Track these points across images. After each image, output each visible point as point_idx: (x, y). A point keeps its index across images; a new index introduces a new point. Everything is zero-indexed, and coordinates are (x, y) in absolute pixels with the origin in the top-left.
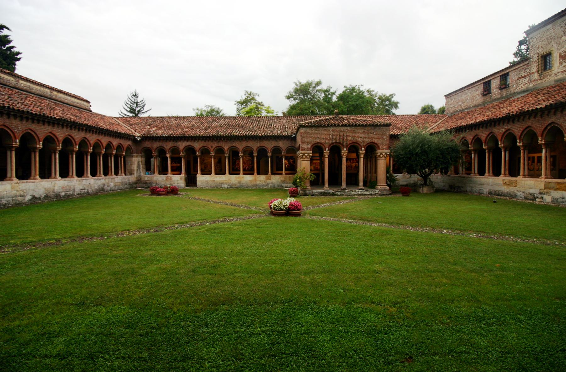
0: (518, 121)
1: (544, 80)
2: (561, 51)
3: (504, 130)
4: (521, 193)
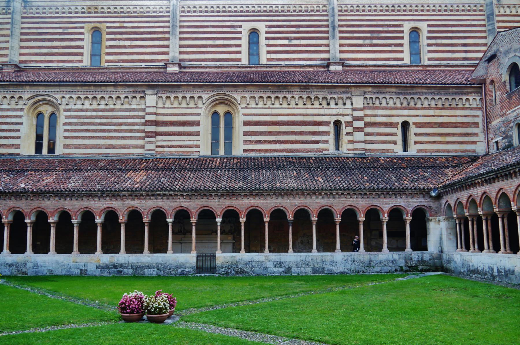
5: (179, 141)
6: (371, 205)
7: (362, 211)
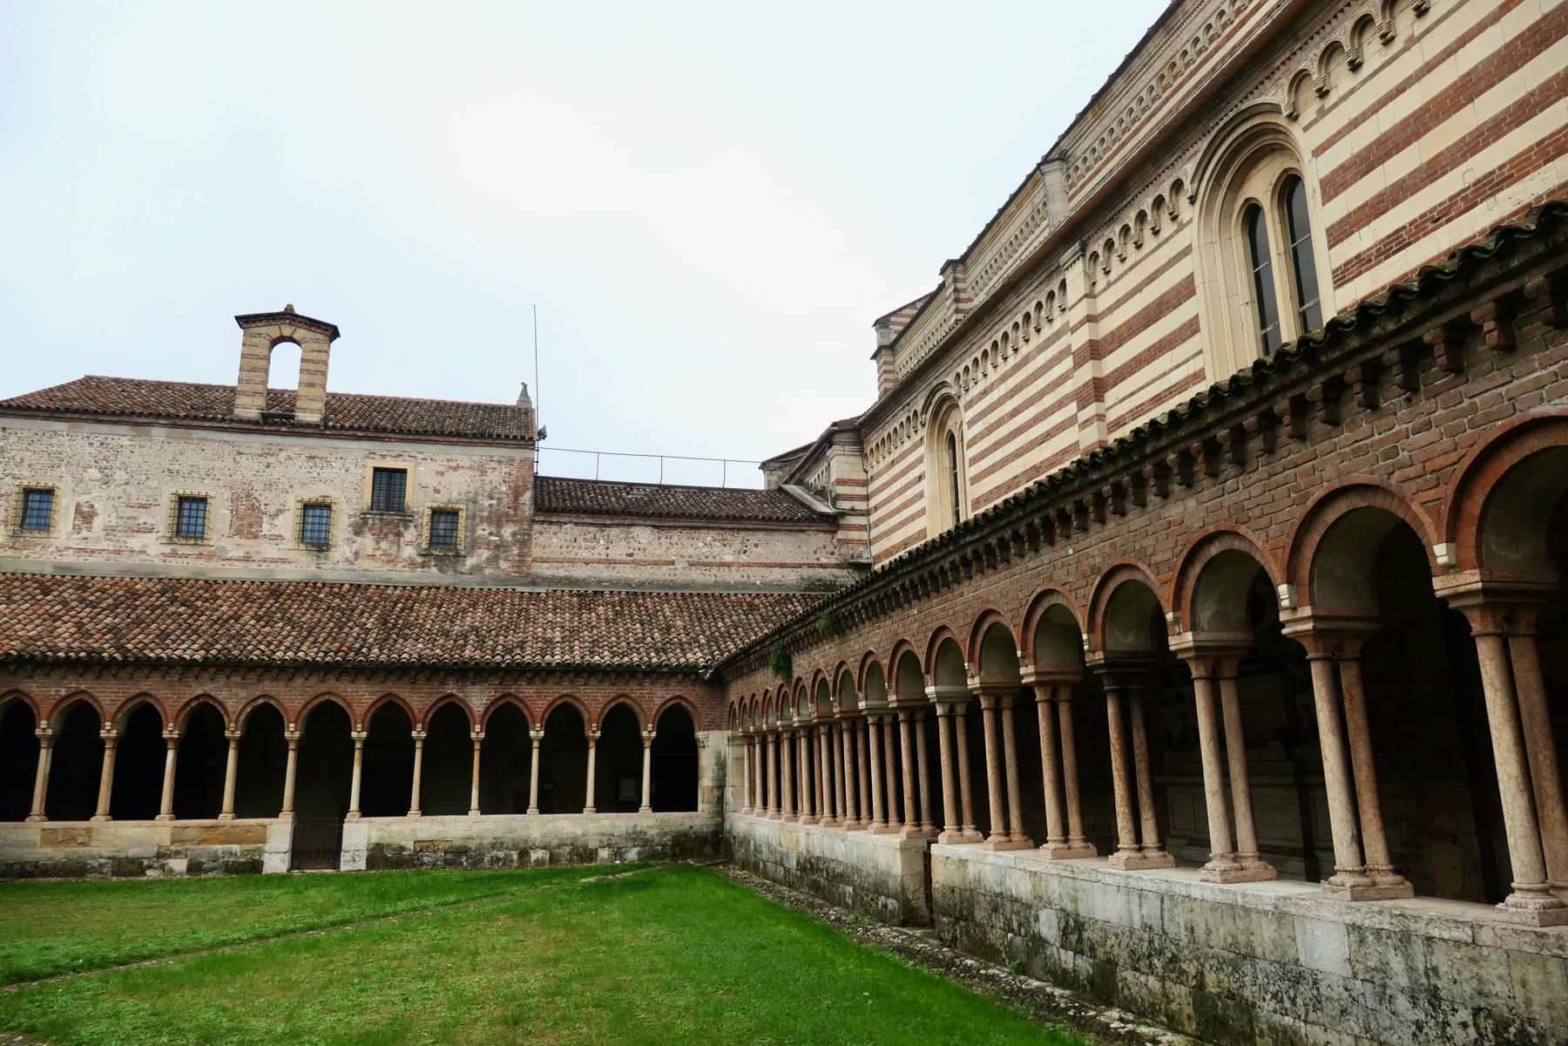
0: (115, 676)
1: (25, 552)
2: (83, 499)
3: (63, 690)
4: (103, 861)
5: (1148, 384)
6: (1499, 426)
7: (1435, 514)
